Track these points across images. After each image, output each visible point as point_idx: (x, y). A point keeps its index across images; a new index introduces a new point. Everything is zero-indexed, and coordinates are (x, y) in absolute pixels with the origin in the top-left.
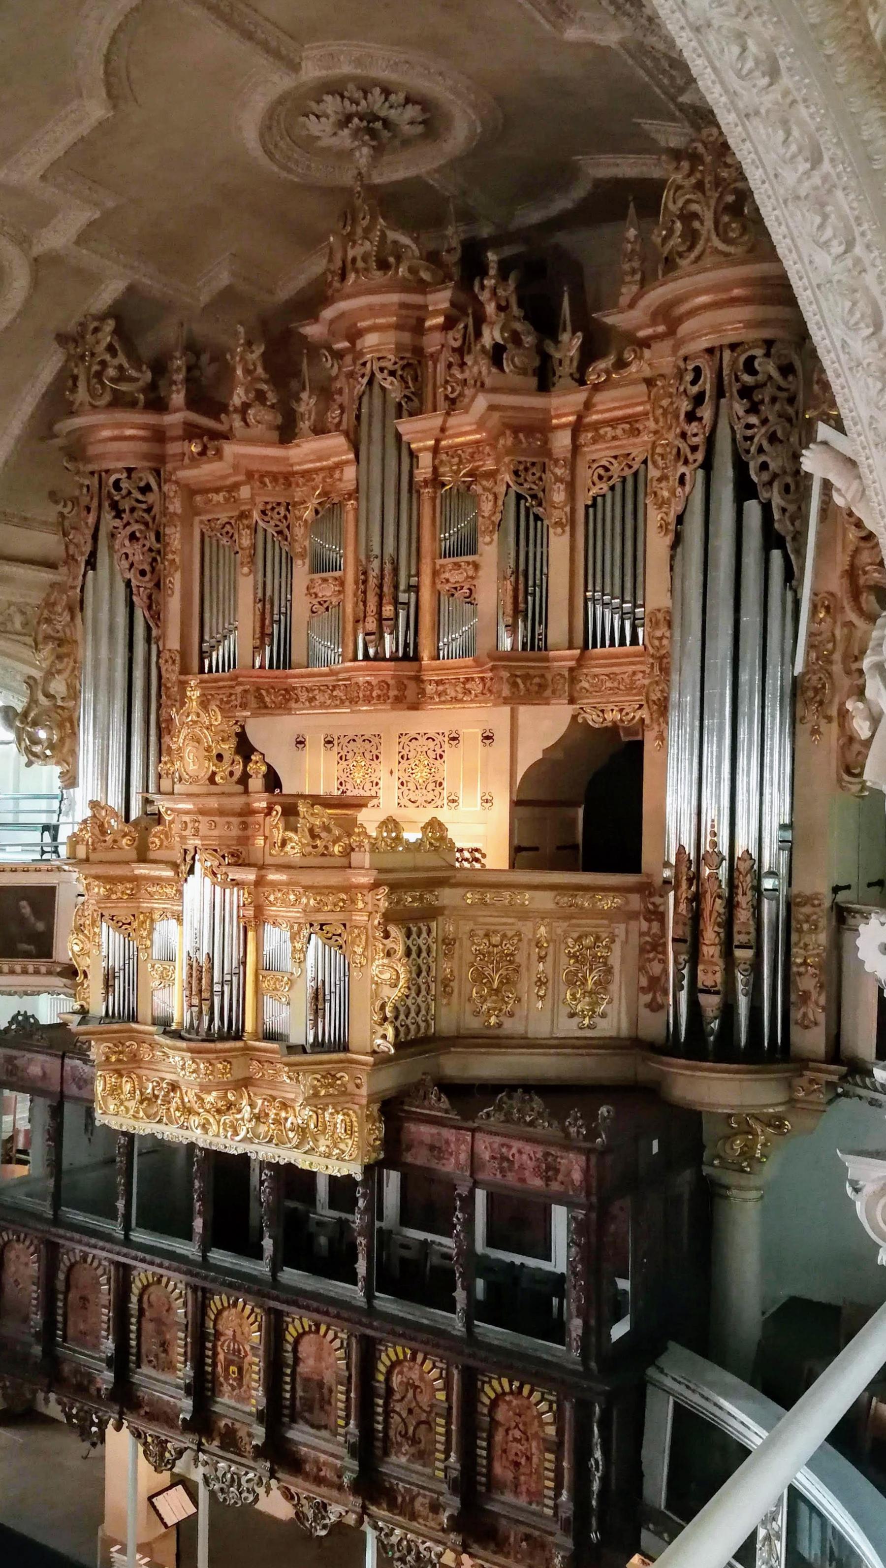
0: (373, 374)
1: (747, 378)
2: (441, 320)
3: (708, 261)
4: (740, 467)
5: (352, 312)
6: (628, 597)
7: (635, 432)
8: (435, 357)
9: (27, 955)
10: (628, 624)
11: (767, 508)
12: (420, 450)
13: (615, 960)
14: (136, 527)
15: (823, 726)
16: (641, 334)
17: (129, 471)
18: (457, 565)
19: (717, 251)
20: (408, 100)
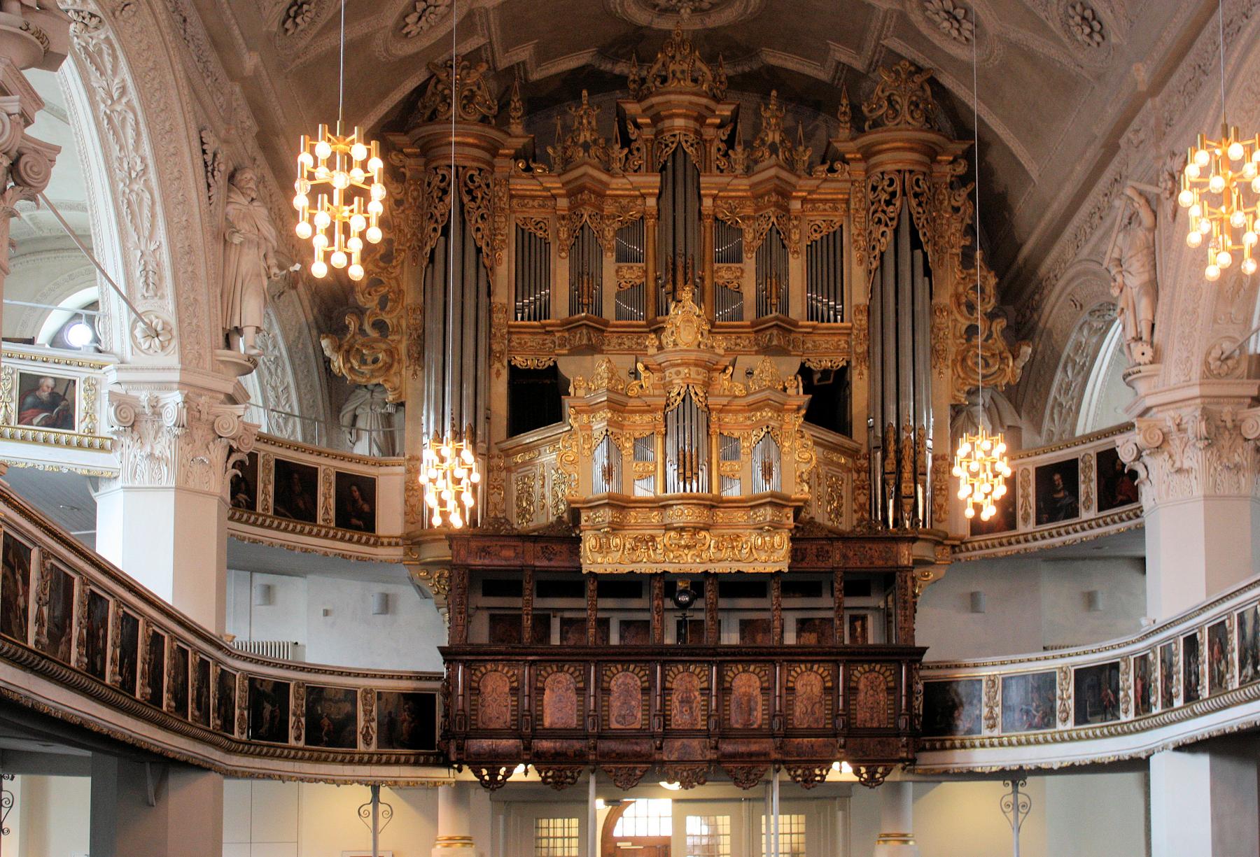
2: (718, 121)
5: (658, 104)
7: (836, 209)
8: (711, 141)
11: (925, 255)
12: (705, 195)
14: (481, 211)
15: (944, 370)
16: (848, 156)
17: (480, 170)
18: (729, 269)
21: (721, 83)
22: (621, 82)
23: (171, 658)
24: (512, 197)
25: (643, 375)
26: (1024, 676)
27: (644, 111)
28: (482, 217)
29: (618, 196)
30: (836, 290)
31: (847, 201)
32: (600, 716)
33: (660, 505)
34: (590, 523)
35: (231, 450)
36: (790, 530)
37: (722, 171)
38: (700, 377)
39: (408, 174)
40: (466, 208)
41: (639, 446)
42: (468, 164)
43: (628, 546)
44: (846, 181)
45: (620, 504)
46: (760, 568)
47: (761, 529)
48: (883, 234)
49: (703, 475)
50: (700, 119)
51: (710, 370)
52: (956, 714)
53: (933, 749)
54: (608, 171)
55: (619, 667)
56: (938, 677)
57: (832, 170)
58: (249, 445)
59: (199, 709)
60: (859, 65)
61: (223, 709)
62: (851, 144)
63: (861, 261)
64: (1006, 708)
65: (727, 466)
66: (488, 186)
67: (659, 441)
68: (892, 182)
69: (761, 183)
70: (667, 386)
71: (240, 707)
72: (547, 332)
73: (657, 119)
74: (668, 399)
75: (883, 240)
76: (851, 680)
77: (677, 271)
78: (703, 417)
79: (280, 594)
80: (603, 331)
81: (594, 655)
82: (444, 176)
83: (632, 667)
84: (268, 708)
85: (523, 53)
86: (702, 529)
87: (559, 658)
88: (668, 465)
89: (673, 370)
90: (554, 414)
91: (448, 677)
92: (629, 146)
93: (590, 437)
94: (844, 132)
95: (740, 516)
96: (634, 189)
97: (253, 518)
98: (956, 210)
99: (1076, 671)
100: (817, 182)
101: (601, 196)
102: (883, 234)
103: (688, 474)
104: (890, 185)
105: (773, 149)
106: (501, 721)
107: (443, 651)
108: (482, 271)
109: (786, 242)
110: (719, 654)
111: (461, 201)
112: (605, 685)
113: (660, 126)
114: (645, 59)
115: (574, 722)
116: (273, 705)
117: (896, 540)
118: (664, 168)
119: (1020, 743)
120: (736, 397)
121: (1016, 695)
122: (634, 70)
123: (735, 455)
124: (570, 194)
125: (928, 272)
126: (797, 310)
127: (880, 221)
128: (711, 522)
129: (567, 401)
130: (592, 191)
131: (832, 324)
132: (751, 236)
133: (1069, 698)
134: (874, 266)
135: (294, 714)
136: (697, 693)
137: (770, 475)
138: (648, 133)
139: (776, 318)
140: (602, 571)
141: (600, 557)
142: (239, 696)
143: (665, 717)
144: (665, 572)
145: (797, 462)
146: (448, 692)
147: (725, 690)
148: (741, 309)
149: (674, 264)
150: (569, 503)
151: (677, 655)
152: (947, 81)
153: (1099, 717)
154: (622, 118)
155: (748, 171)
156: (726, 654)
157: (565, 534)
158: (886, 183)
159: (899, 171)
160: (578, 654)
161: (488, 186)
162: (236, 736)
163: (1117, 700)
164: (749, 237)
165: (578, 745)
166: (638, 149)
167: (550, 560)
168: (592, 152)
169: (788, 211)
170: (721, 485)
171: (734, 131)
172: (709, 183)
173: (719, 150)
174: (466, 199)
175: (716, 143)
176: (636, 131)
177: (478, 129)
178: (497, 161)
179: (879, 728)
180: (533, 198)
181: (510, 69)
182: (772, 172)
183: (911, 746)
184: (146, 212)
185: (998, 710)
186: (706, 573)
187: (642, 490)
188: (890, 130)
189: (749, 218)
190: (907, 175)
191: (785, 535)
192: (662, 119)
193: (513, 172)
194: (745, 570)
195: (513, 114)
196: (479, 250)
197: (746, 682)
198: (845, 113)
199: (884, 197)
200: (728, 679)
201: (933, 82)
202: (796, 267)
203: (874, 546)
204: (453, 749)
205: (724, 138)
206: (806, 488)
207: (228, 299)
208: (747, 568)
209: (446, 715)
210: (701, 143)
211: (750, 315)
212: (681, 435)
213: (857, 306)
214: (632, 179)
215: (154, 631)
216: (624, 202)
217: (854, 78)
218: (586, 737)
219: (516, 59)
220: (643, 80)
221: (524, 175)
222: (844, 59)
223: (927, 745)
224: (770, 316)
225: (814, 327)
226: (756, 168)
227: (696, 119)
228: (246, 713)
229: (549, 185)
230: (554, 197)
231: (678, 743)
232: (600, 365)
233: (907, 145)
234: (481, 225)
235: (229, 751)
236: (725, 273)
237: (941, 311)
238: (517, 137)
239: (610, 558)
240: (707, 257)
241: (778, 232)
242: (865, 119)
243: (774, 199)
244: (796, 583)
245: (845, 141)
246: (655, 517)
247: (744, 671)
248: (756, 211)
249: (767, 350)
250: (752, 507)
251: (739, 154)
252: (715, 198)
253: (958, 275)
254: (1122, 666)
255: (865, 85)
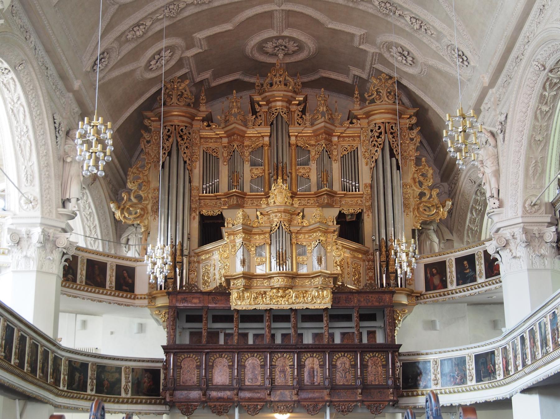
0: (279, 112)
1: (392, 130)
2: (298, 102)
3: (383, 102)
4: (391, 150)
6: (354, 181)
7: (354, 140)
9: (126, 291)
10: (354, 188)
11: (397, 160)
12: (292, 136)
13: (361, 272)
14: (186, 145)
16: (359, 116)
17: (186, 127)
19: (385, 101)
20: (297, 46)
21: (299, 85)
22: (251, 86)
23: (29, 347)
24: (201, 138)
25: (260, 217)
26: (451, 359)
27: (262, 99)
28: (187, 147)
29: (251, 137)
30: (356, 177)
31: (359, 137)
32: (240, 380)
33: (268, 277)
34: (235, 286)
35: (64, 254)
36: (332, 289)
37: (300, 125)
38: (287, 218)
39: (153, 129)
40: (179, 144)
41: (259, 250)
42: (180, 124)
43: (253, 297)
44: (358, 128)
45: (249, 277)
46: (317, 306)
47: (317, 288)
48: (376, 151)
49: (289, 263)
50: (289, 102)
51: (291, 214)
52: (419, 378)
53: (408, 396)
54: (246, 125)
55: (249, 354)
56: (408, 360)
57: (351, 123)
58: (72, 252)
59: (43, 372)
60: (365, 76)
61: (55, 375)
62: (360, 111)
63: (367, 164)
64: (442, 375)
65: (301, 259)
66: (190, 133)
67: (268, 247)
68: (380, 128)
69: (317, 130)
70: (271, 222)
71: (63, 374)
72: (217, 199)
73: (268, 102)
74: (271, 228)
75: (376, 154)
76: (363, 361)
77: (279, 171)
78: (288, 236)
79: (89, 325)
80: (244, 198)
81: (237, 349)
82: (169, 130)
83: (256, 355)
84: (77, 375)
85: (207, 75)
86: (288, 288)
87: (221, 351)
88: (272, 258)
89: (274, 215)
90: (219, 237)
91: (166, 360)
92: (256, 115)
93: (235, 246)
94: (357, 107)
95: (307, 282)
96: (258, 133)
97: (75, 286)
98: (412, 139)
99: (475, 356)
100: (345, 128)
101: (243, 137)
102: (376, 151)
103: (281, 262)
104: (379, 129)
105: (323, 114)
106: (191, 382)
107: (163, 347)
108: (187, 172)
109: (330, 156)
110: (298, 348)
111: (177, 141)
112: (243, 363)
113: (270, 105)
114: (265, 76)
115: (227, 382)
116: (80, 374)
117: (384, 292)
118: (272, 124)
119: (450, 393)
120: (304, 226)
121: (447, 369)
122: (258, 81)
123: (304, 253)
124: (228, 136)
125: (398, 168)
126: (337, 187)
127: (375, 145)
128: (293, 285)
129: (224, 230)
130: (238, 135)
131: (354, 192)
132: (314, 153)
133: (473, 369)
134: (373, 166)
135: (90, 378)
136: (288, 368)
137: (321, 262)
138: (265, 109)
139: (326, 190)
140: (240, 309)
141: (240, 302)
142: (63, 368)
143: (272, 380)
144: (271, 309)
145: (334, 256)
146: (166, 368)
147: (301, 366)
148: (310, 187)
149: (277, 166)
150: (225, 276)
151: (277, 349)
152: (404, 82)
153: (487, 378)
154: (252, 103)
155: (312, 125)
156: (301, 348)
157: (223, 292)
158: (377, 128)
159: (383, 123)
160: (229, 349)
161: (190, 133)
162: (61, 388)
163: (495, 369)
164: (313, 153)
165: (228, 394)
166: (260, 116)
167: (216, 304)
168: (238, 118)
169: (331, 142)
170: (297, 268)
171: (305, 107)
172: (293, 130)
173: (298, 115)
174: (179, 139)
175: (297, 112)
176: (259, 108)
177: (184, 109)
178: (194, 123)
179: (379, 385)
180: (211, 138)
181: (201, 82)
182: (323, 124)
183: (395, 394)
184: (28, 149)
185: (439, 376)
186: (291, 309)
187: (260, 270)
188: (378, 105)
189: (313, 145)
190: (387, 124)
191: (329, 291)
192: (271, 102)
193: (201, 127)
194: (310, 308)
195: (201, 102)
196: (185, 162)
197: (312, 362)
198: (357, 98)
199: (377, 134)
200: (303, 360)
201: (399, 83)
202: (336, 167)
203: (374, 296)
204: (168, 395)
205: (300, 110)
206: (339, 268)
207: (63, 187)
208: (311, 307)
209: (165, 379)
210: (289, 112)
211: (314, 190)
212: (278, 244)
213: (365, 184)
214: (257, 129)
215: (22, 334)
216: (254, 139)
217: (362, 83)
218: (233, 389)
219: (203, 78)
220: (262, 85)
221: (207, 128)
222: (357, 73)
223: (405, 394)
224: (323, 189)
225: (345, 194)
226: (316, 123)
227: (287, 102)
228: (66, 377)
229: (218, 133)
230: (221, 138)
231: (278, 392)
232: (240, 213)
233: (386, 111)
234: (186, 151)
235: (57, 395)
236: (302, 170)
237: (406, 186)
238: (203, 112)
239: (243, 303)
240: (293, 163)
241: (326, 151)
242: (366, 100)
243: (324, 136)
244: (336, 315)
245: (357, 110)
246: (266, 283)
247: (311, 357)
248: (316, 142)
249: (322, 206)
250: (313, 278)
251: (308, 116)
252: (296, 136)
253: (414, 169)
254: (496, 352)
255: (368, 85)
